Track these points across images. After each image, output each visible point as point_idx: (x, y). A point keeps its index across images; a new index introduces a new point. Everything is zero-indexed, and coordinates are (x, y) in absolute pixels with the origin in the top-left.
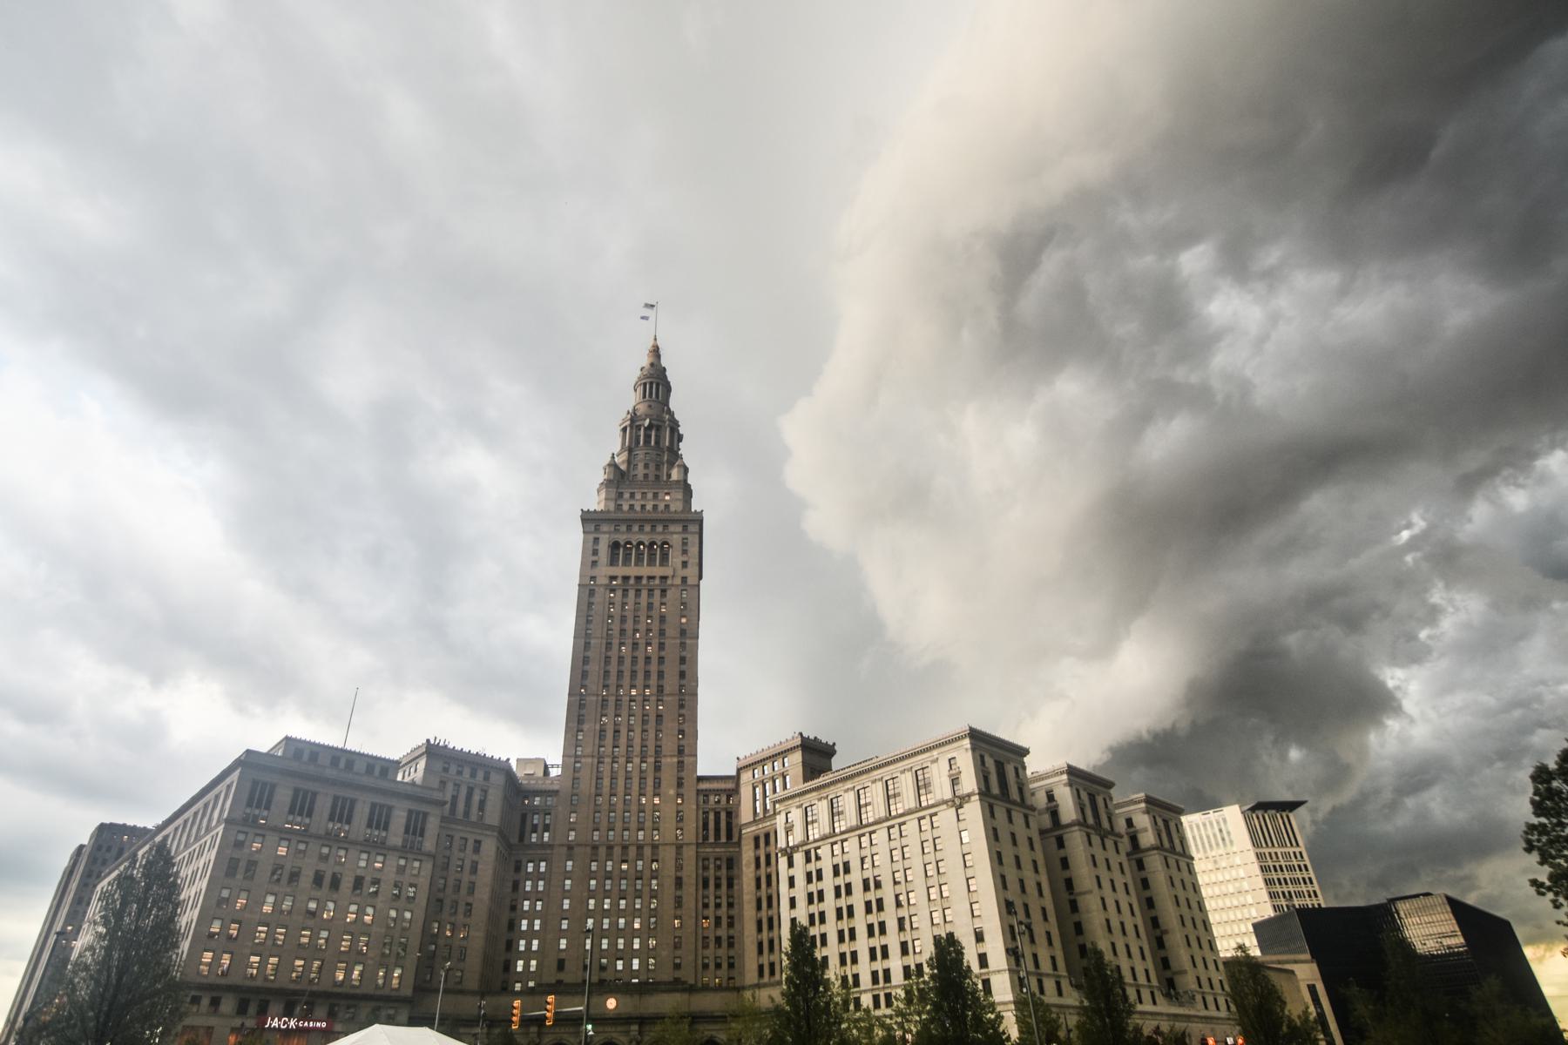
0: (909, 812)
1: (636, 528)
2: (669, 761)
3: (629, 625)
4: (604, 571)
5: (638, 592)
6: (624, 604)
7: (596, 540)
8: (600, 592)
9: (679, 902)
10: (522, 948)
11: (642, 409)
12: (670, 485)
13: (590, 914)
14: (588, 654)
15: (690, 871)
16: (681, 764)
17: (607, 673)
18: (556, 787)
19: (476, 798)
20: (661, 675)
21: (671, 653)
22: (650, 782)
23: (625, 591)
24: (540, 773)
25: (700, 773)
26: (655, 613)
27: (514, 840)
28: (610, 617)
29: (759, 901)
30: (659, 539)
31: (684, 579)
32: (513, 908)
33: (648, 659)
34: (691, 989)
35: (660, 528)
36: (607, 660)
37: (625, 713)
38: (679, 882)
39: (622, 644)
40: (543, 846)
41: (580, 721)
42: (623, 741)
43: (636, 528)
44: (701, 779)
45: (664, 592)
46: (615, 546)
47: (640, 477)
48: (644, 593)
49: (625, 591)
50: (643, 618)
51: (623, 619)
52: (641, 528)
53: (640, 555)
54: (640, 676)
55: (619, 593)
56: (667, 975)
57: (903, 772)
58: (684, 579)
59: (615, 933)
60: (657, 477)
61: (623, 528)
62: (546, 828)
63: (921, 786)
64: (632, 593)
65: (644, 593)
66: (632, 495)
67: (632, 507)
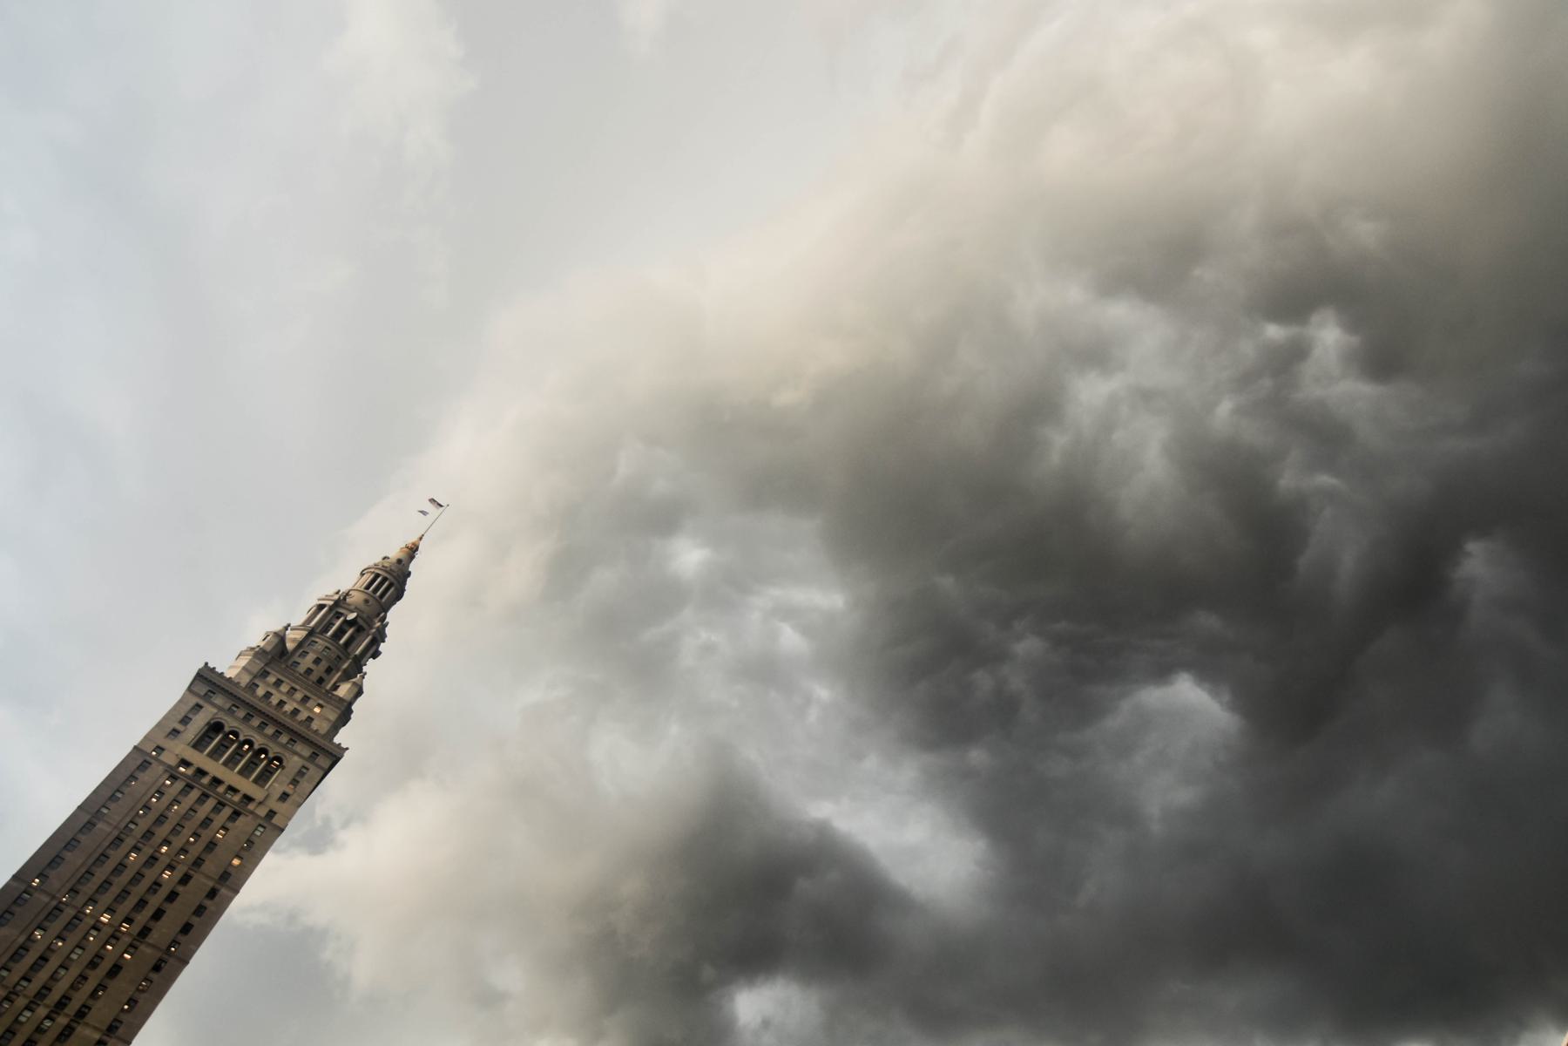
1: (256, 722)
3: (163, 831)
5: (204, 796)
6: (176, 801)
11: (356, 598)
12: (329, 697)
14: (82, 838)
20: (158, 914)
21: (192, 895)
26: (206, 835)
28: (147, 807)
30: (274, 750)
39: (136, 849)
43: (256, 722)
47: (302, 669)
49: (190, 787)
50: (186, 832)
51: (161, 819)
52: (263, 726)
53: (238, 754)
55: (179, 785)
60: (321, 681)
61: (241, 713)
66: (278, 683)
67: (268, 695)
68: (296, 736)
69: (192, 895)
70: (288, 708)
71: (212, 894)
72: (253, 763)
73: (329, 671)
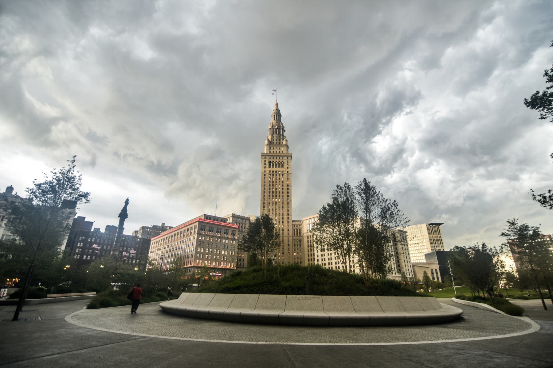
1: (275, 158)
2: (285, 217)
3: (274, 183)
4: (267, 169)
5: (276, 175)
7: (265, 161)
8: (267, 175)
9: (289, 249)
15: (291, 242)
16: (288, 218)
17: (270, 196)
19: (244, 226)
21: (285, 191)
22: (281, 222)
23: (273, 175)
25: (293, 219)
26: (281, 180)
30: (281, 161)
31: (288, 172)
33: (279, 192)
35: (281, 158)
36: (270, 192)
37: (274, 205)
38: (289, 245)
41: (264, 207)
42: (274, 212)
43: (275, 158)
44: (293, 221)
45: (283, 175)
46: (270, 162)
48: (278, 175)
49: (273, 175)
51: (273, 182)
53: (276, 166)
54: (278, 196)
58: (288, 172)
60: (279, 143)
64: (275, 175)
65: (278, 175)
68: (283, 156)
69: (285, 191)
70: (278, 152)
71: (288, 189)
72: (279, 166)
73: (279, 140)
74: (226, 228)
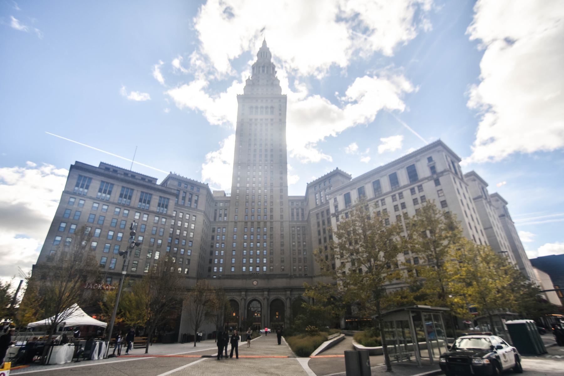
0: (405, 187)
10: (216, 262)
13: (244, 249)
18: (229, 199)
24: (223, 195)
27: (212, 220)
29: (320, 240)
32: (212, 246)
34: (290, 277)
40: (225, 222)
46: (251, 107)
56: (278, 272)
57: (398, 169)
59: (255, 256)
62: (225, 215)
63: (413, 174)
74: (145, 190)
